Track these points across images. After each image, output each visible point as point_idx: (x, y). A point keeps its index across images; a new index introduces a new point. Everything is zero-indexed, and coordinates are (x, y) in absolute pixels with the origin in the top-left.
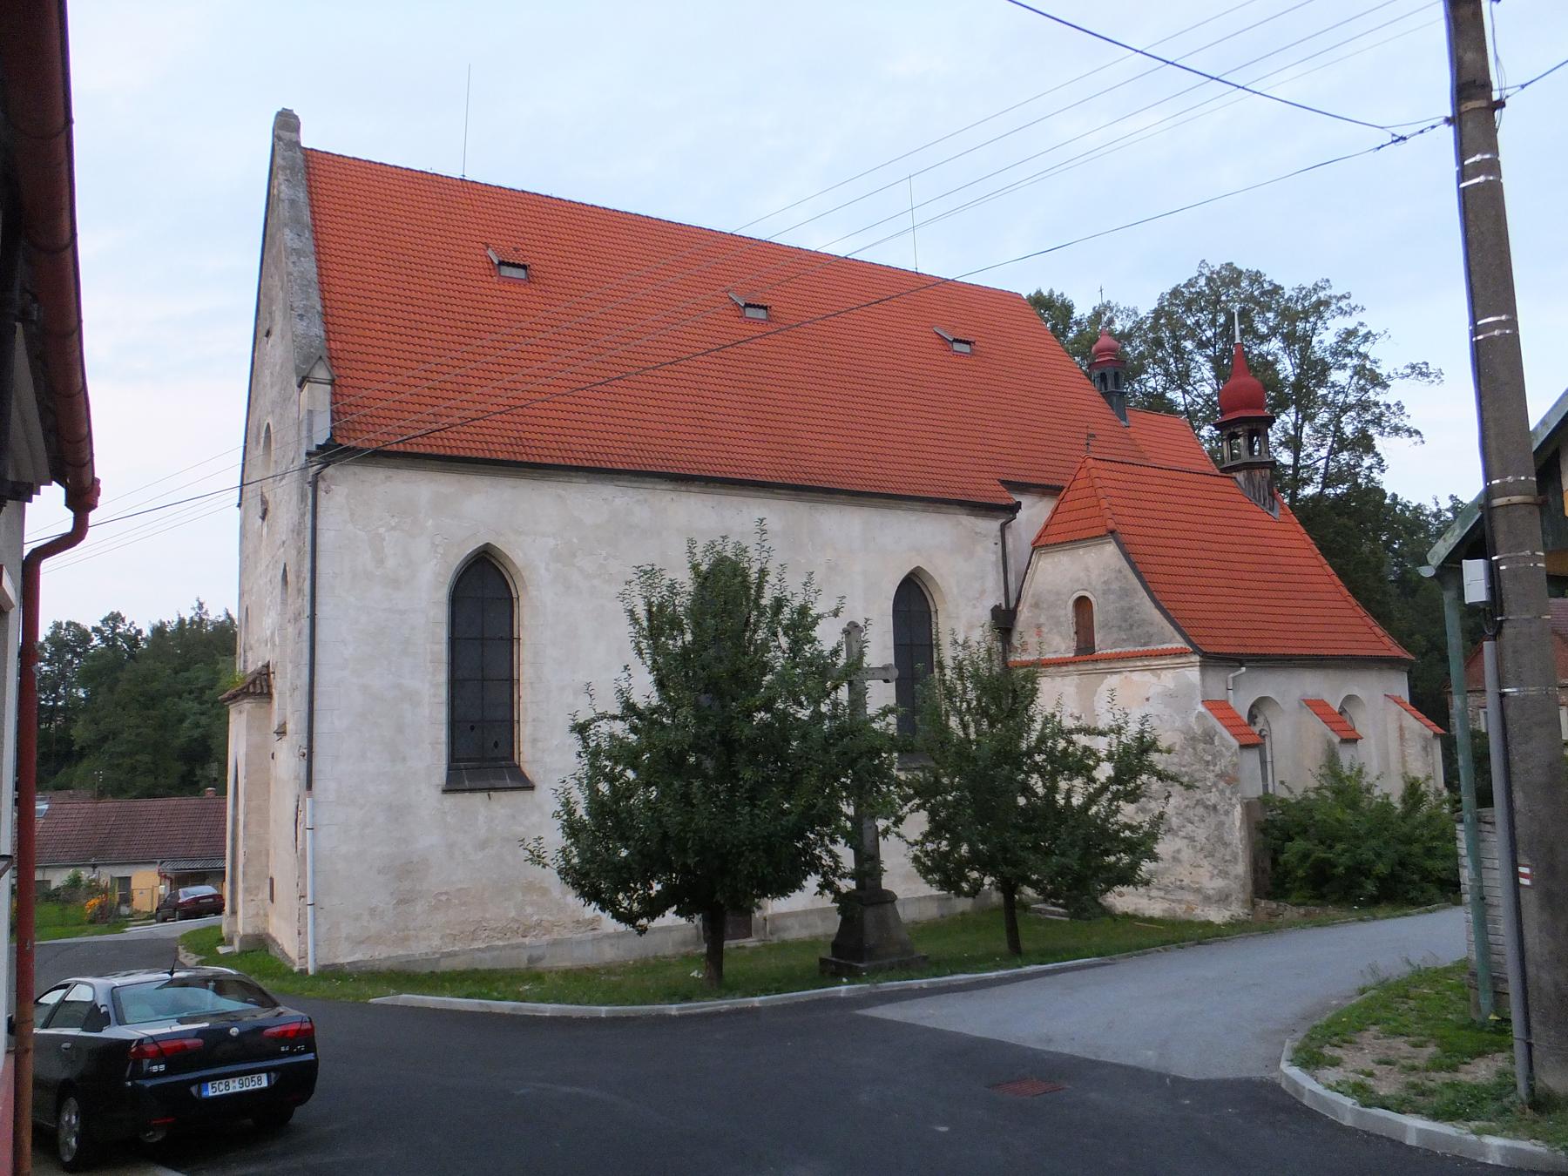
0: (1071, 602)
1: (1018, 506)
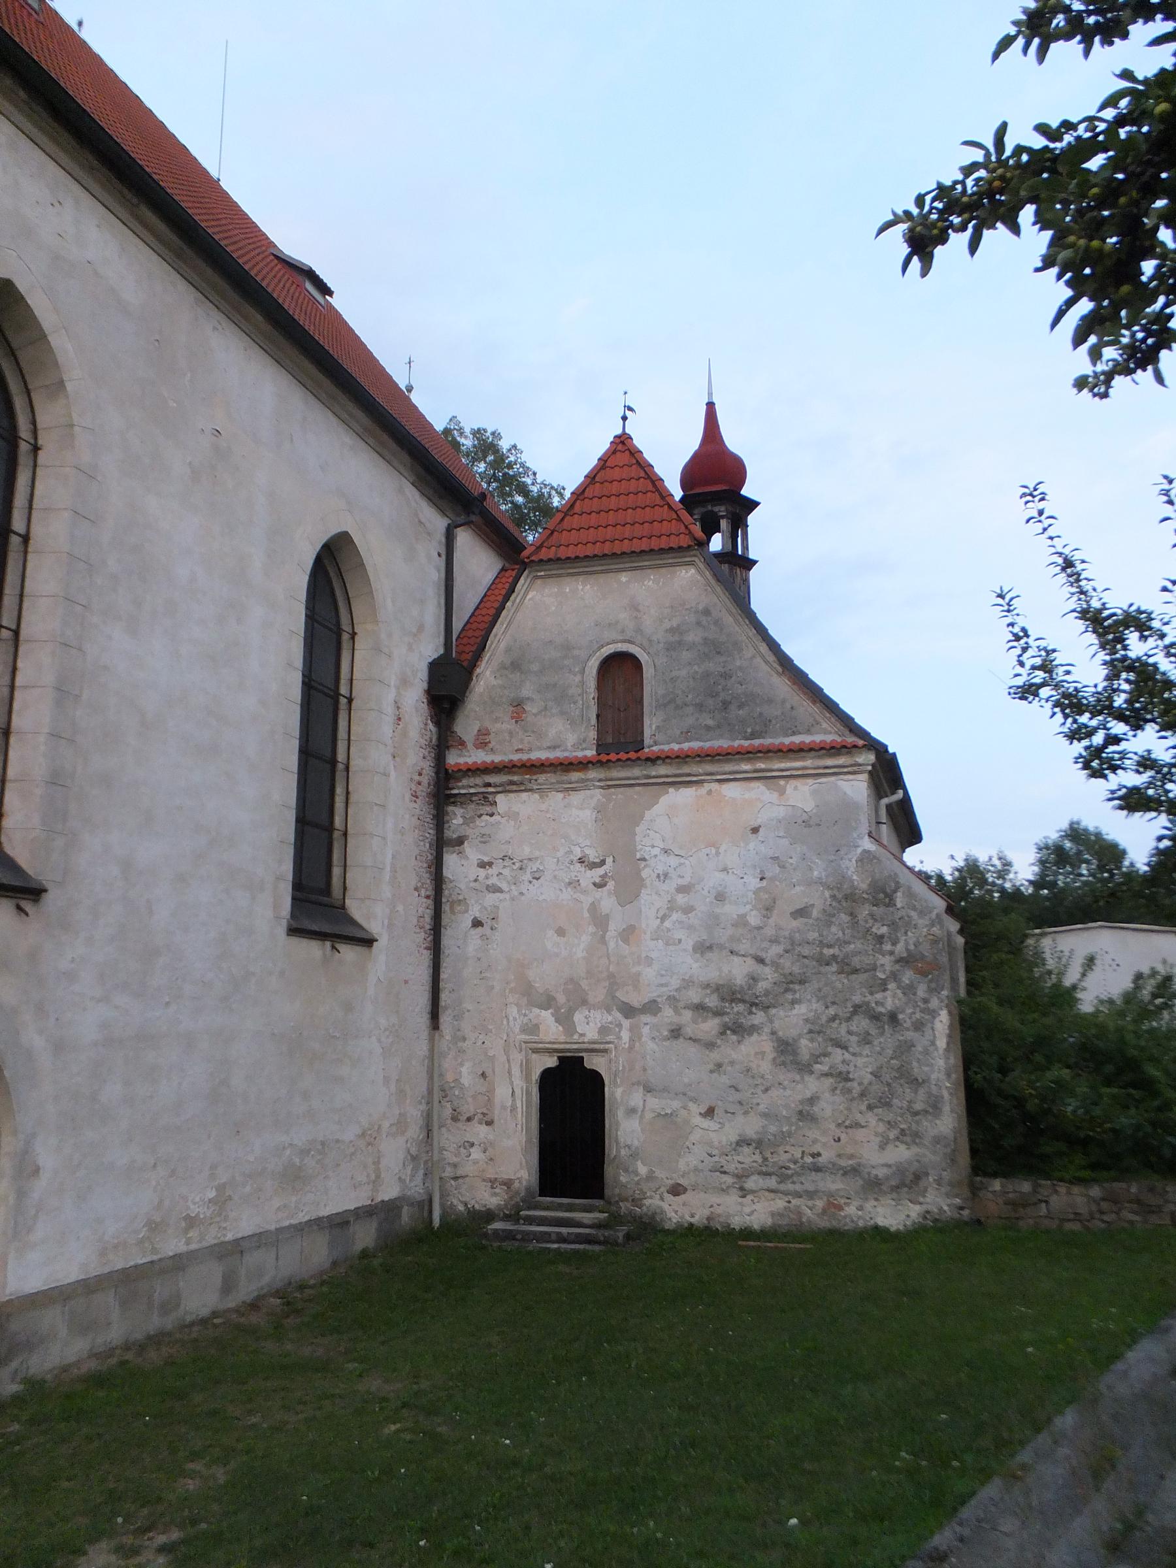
0: (594, 665)
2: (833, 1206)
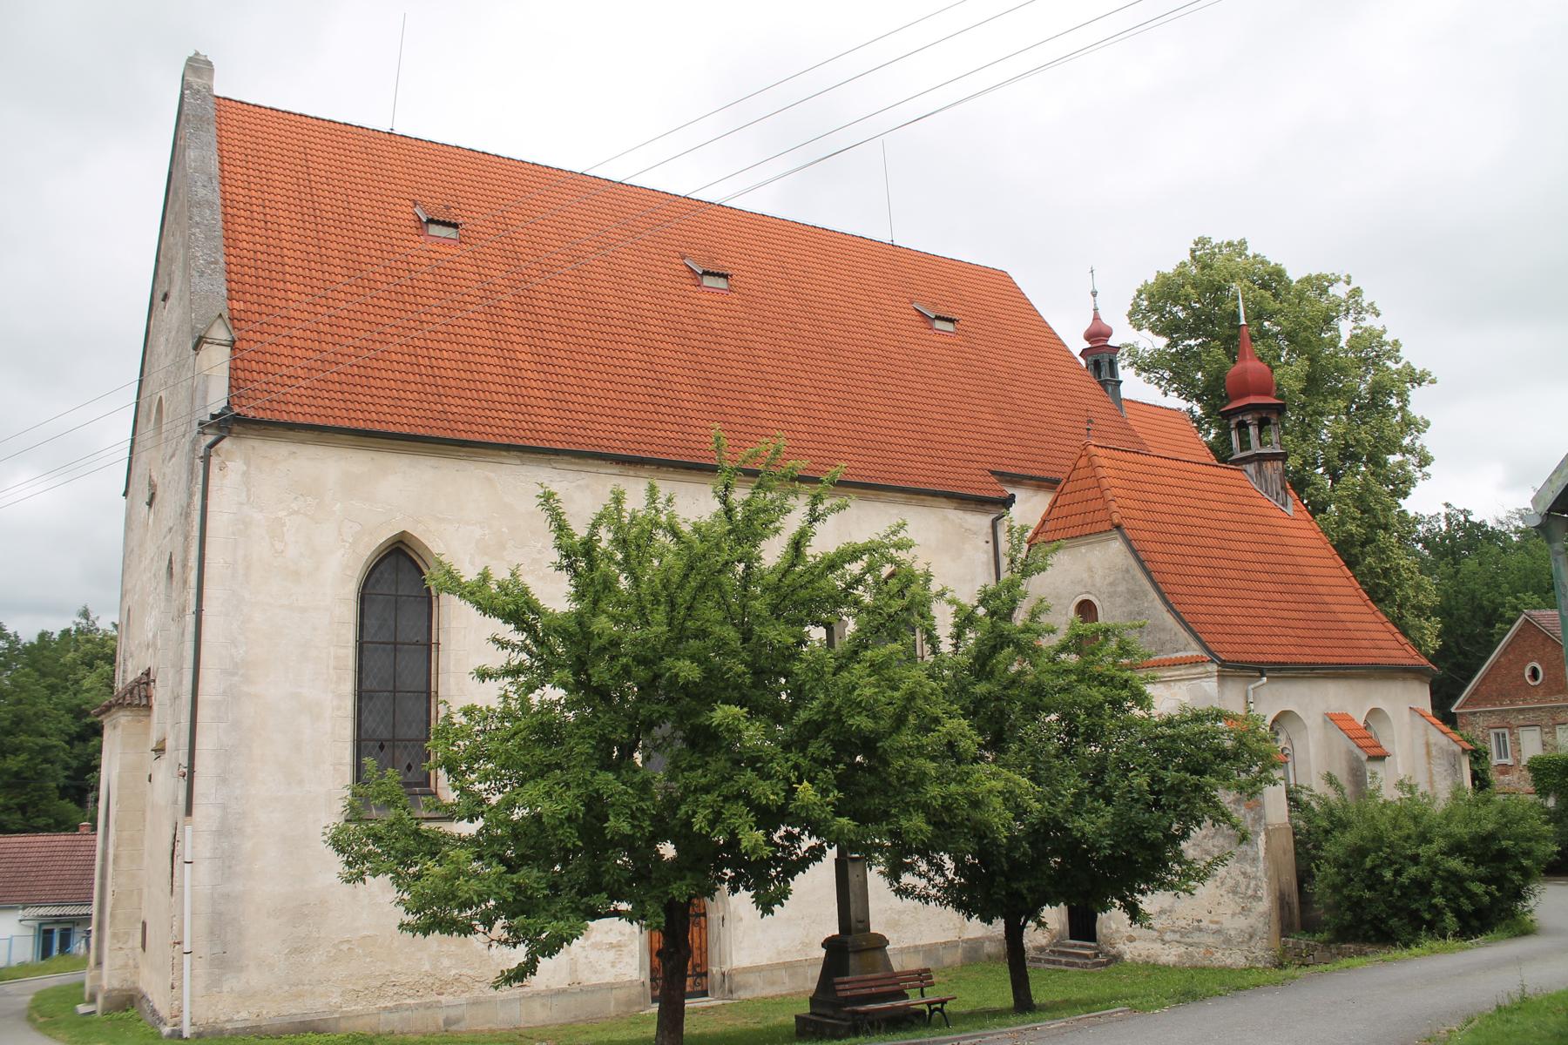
0: (1072, 608)
1: (1012, 499)
2: (1209, 952)
